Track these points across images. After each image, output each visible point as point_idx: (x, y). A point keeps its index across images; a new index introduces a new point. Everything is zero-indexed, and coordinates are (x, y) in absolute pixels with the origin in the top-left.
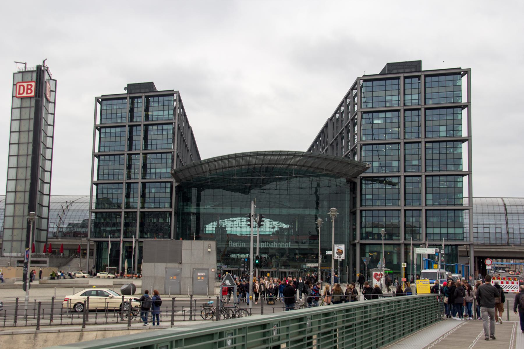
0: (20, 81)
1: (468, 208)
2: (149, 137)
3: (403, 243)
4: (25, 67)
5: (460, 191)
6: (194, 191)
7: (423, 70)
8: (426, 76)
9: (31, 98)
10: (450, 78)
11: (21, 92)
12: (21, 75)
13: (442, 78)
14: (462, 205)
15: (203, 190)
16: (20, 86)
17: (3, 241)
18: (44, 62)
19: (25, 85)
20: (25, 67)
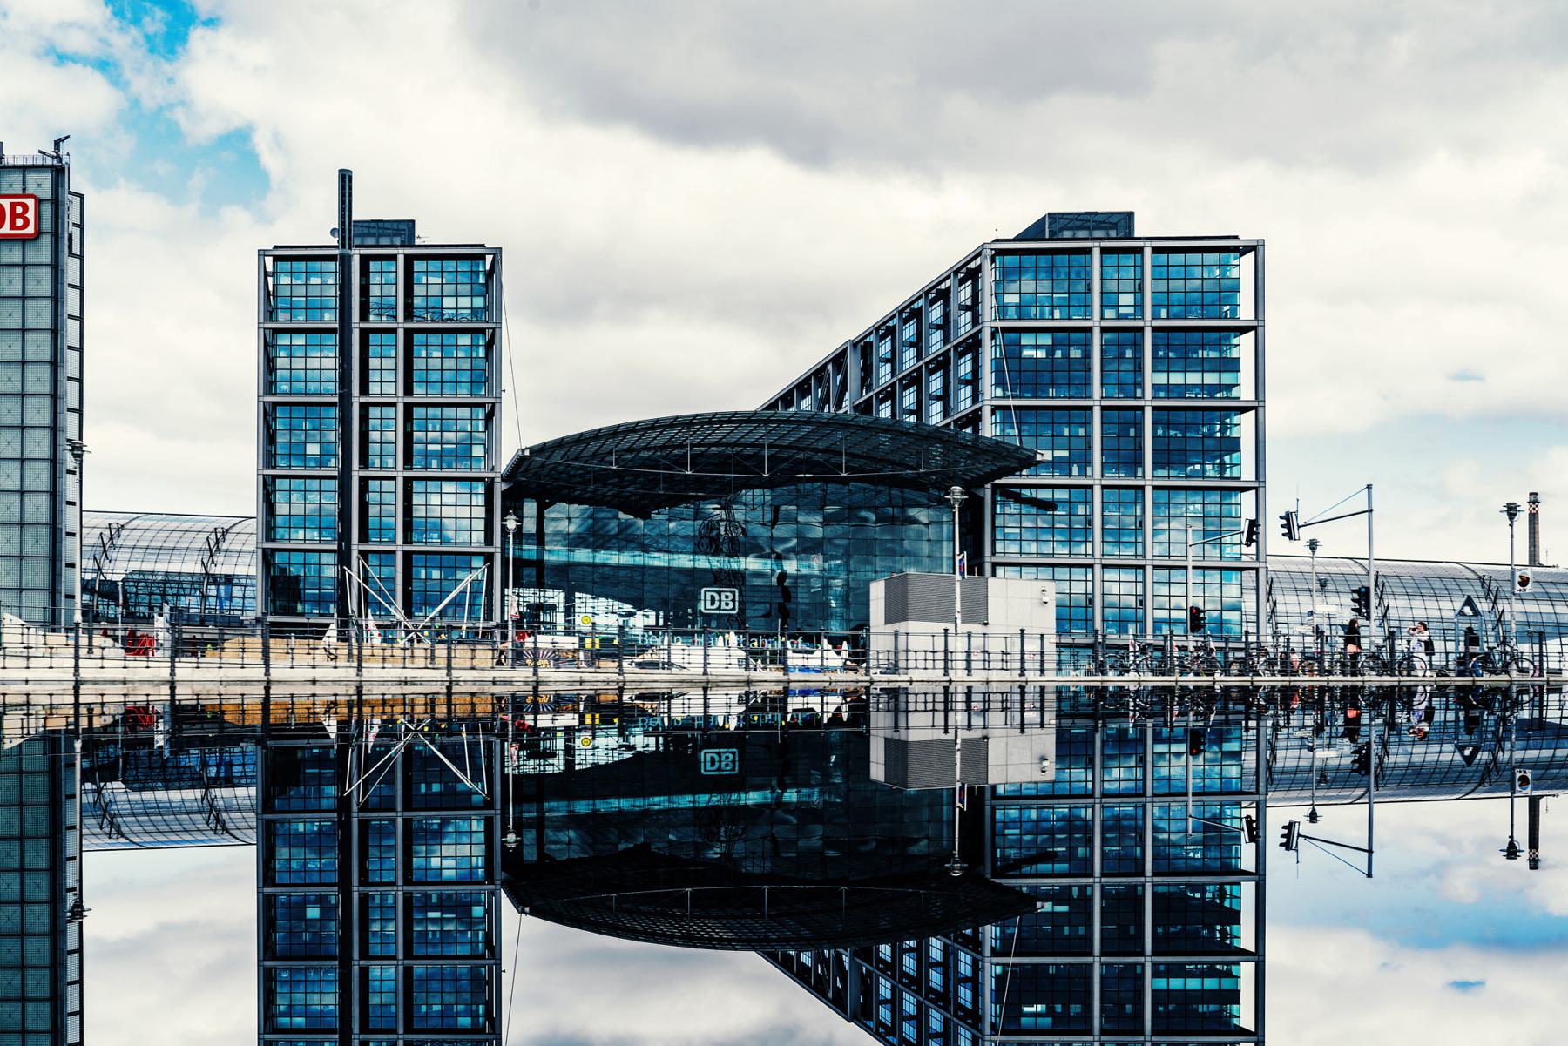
2: (418, 364)
9: (24, 240)
10: (1212, 258)
13: (1194, 258)
18: (57, 144)
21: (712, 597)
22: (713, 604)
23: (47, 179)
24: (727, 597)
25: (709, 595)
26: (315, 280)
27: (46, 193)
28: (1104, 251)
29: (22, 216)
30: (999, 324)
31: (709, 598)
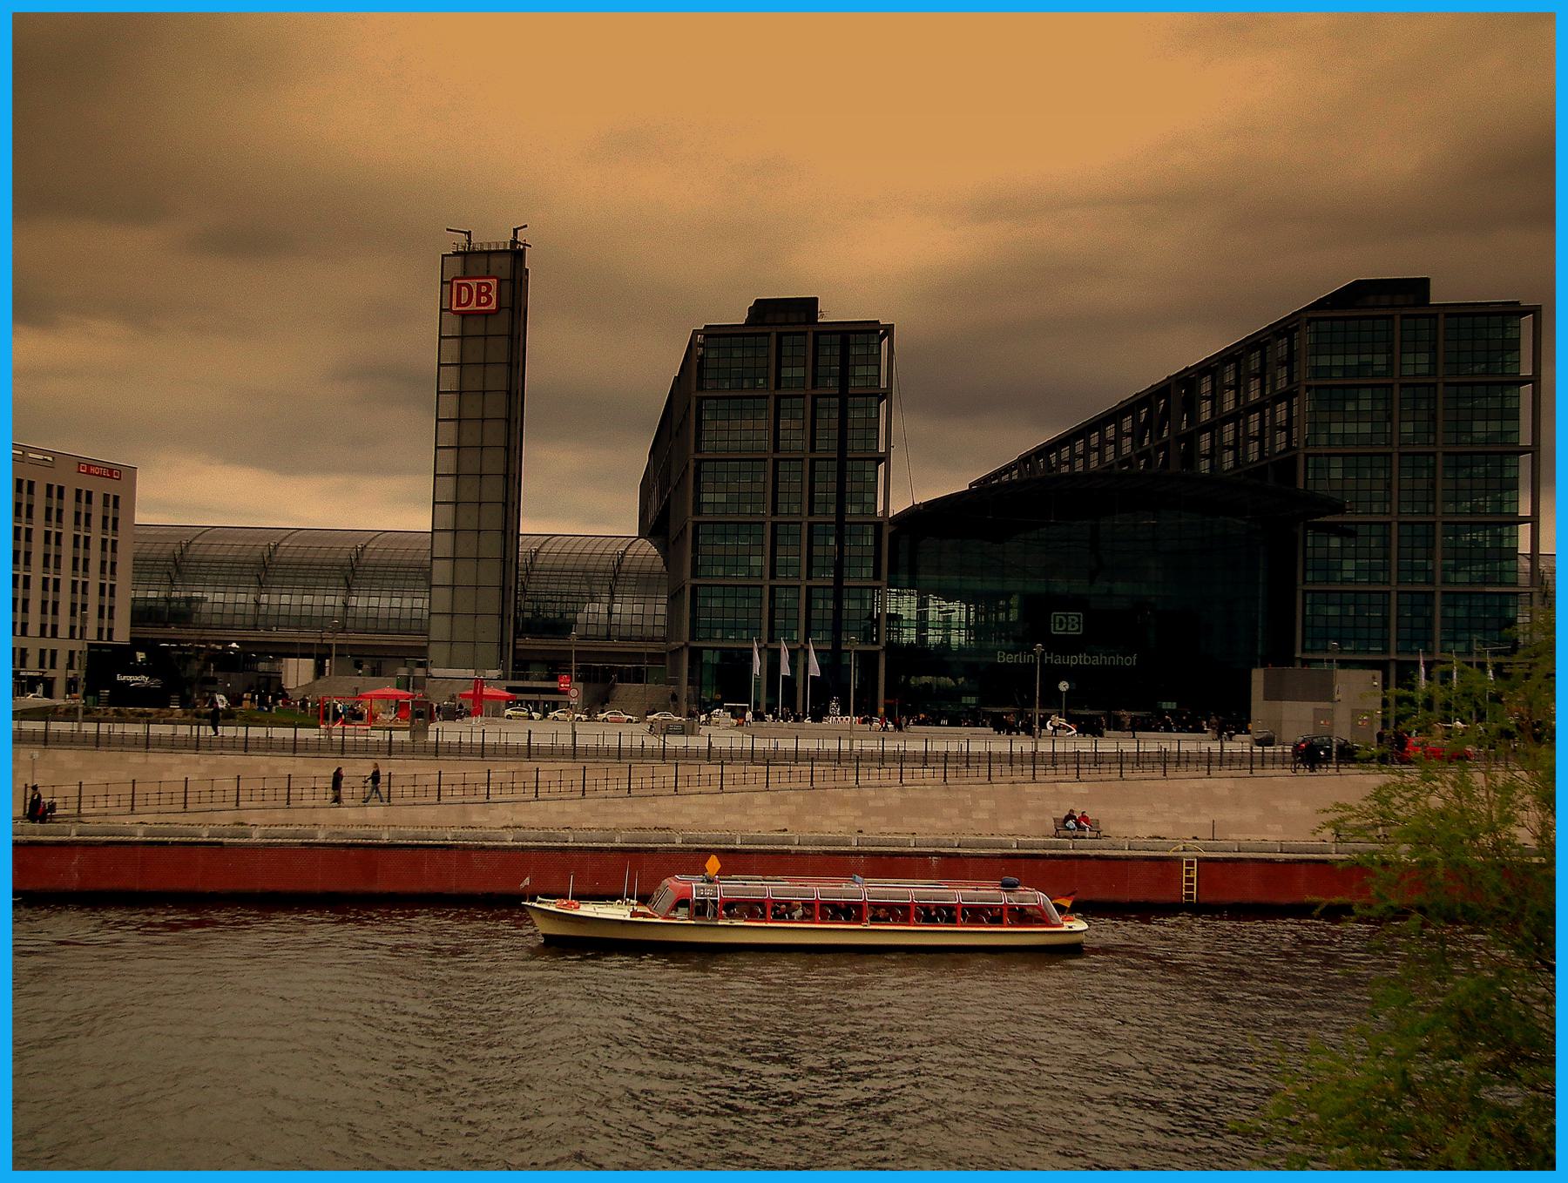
0: (458, 275)
1: (1531, 590)
3: (1393, 660)
4: (469, 241)
5: (1513, 553)
7: (1434, 300)
8: (1447, 315)
9: (487, 314)
14: (1515, 584)
16: (460, 286)
17: (429, 642)
18: (515, 231)
19: (473, 283)
20: (469, 241)
21: (1061, 620)
22: (1061, 626)
23: (506, 262)
24: (1073, 620)
26: (737, 354)
27: (506, 274)
28: (1403, 317)
29: (486, 294)
30: (1313, 383)
31: (1057, 621)
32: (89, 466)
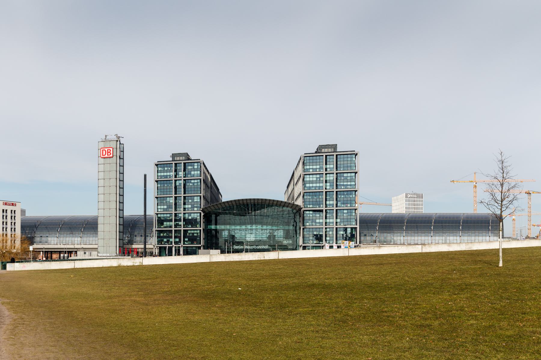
0: (102, 147)
6: (213, 217)
9: (110, 157)
11: (104, 154)
12: (103, 142)
15: (219, 215)
16: (103, 150)
19: (106, 149)
25: (248, 236)
32: (6, 203)
